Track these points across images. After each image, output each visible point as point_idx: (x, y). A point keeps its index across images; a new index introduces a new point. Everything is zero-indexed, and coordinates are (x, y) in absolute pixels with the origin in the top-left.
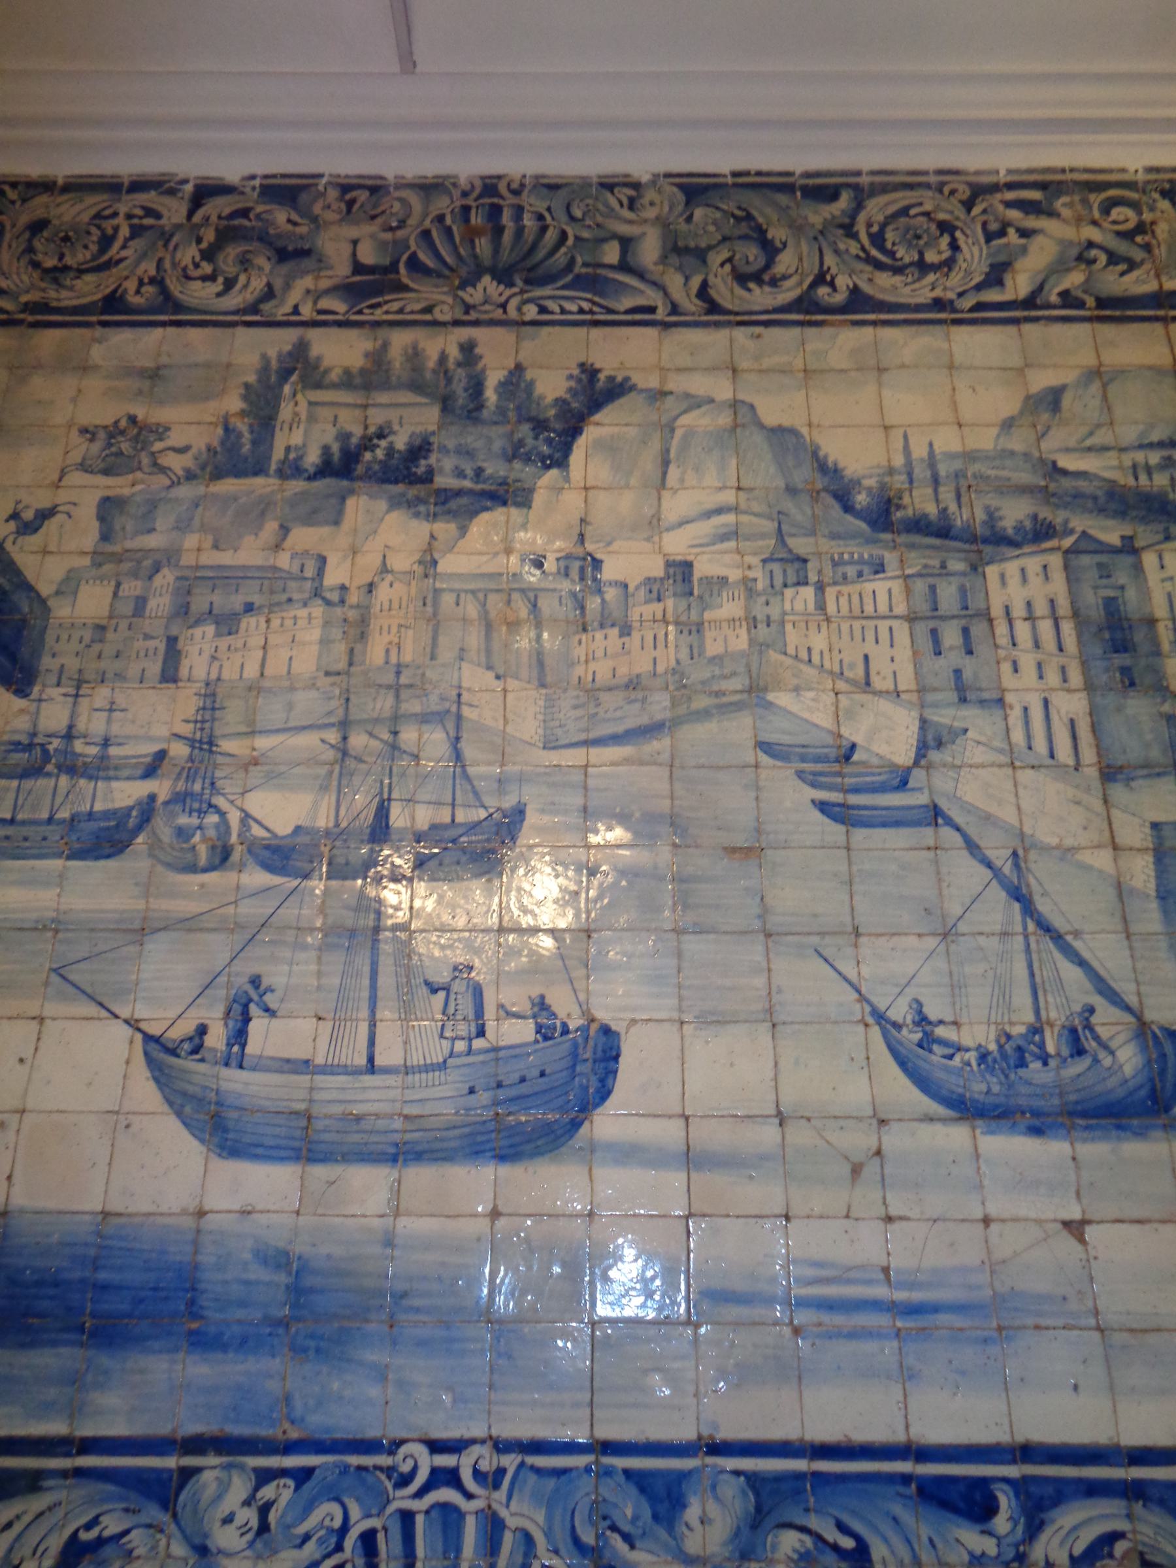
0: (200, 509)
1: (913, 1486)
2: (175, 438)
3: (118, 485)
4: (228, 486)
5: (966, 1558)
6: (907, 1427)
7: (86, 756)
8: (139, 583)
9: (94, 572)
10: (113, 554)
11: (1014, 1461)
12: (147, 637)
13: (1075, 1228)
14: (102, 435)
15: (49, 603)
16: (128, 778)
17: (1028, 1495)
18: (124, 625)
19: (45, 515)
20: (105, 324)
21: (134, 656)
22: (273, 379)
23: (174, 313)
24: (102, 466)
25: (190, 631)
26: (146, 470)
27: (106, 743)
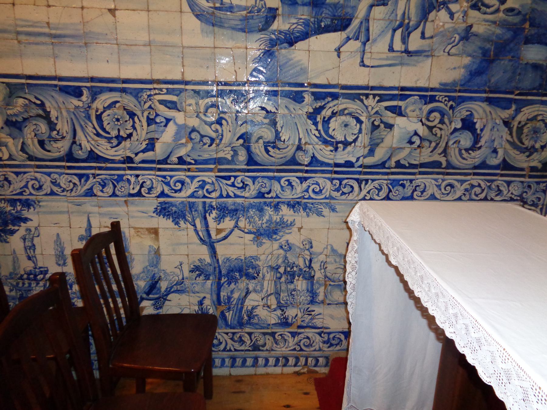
1: (58, 88)
5: (74, 107)
6: (55, 71)
11: (88, 82)
13: (112, 11)
17: (92, 91)
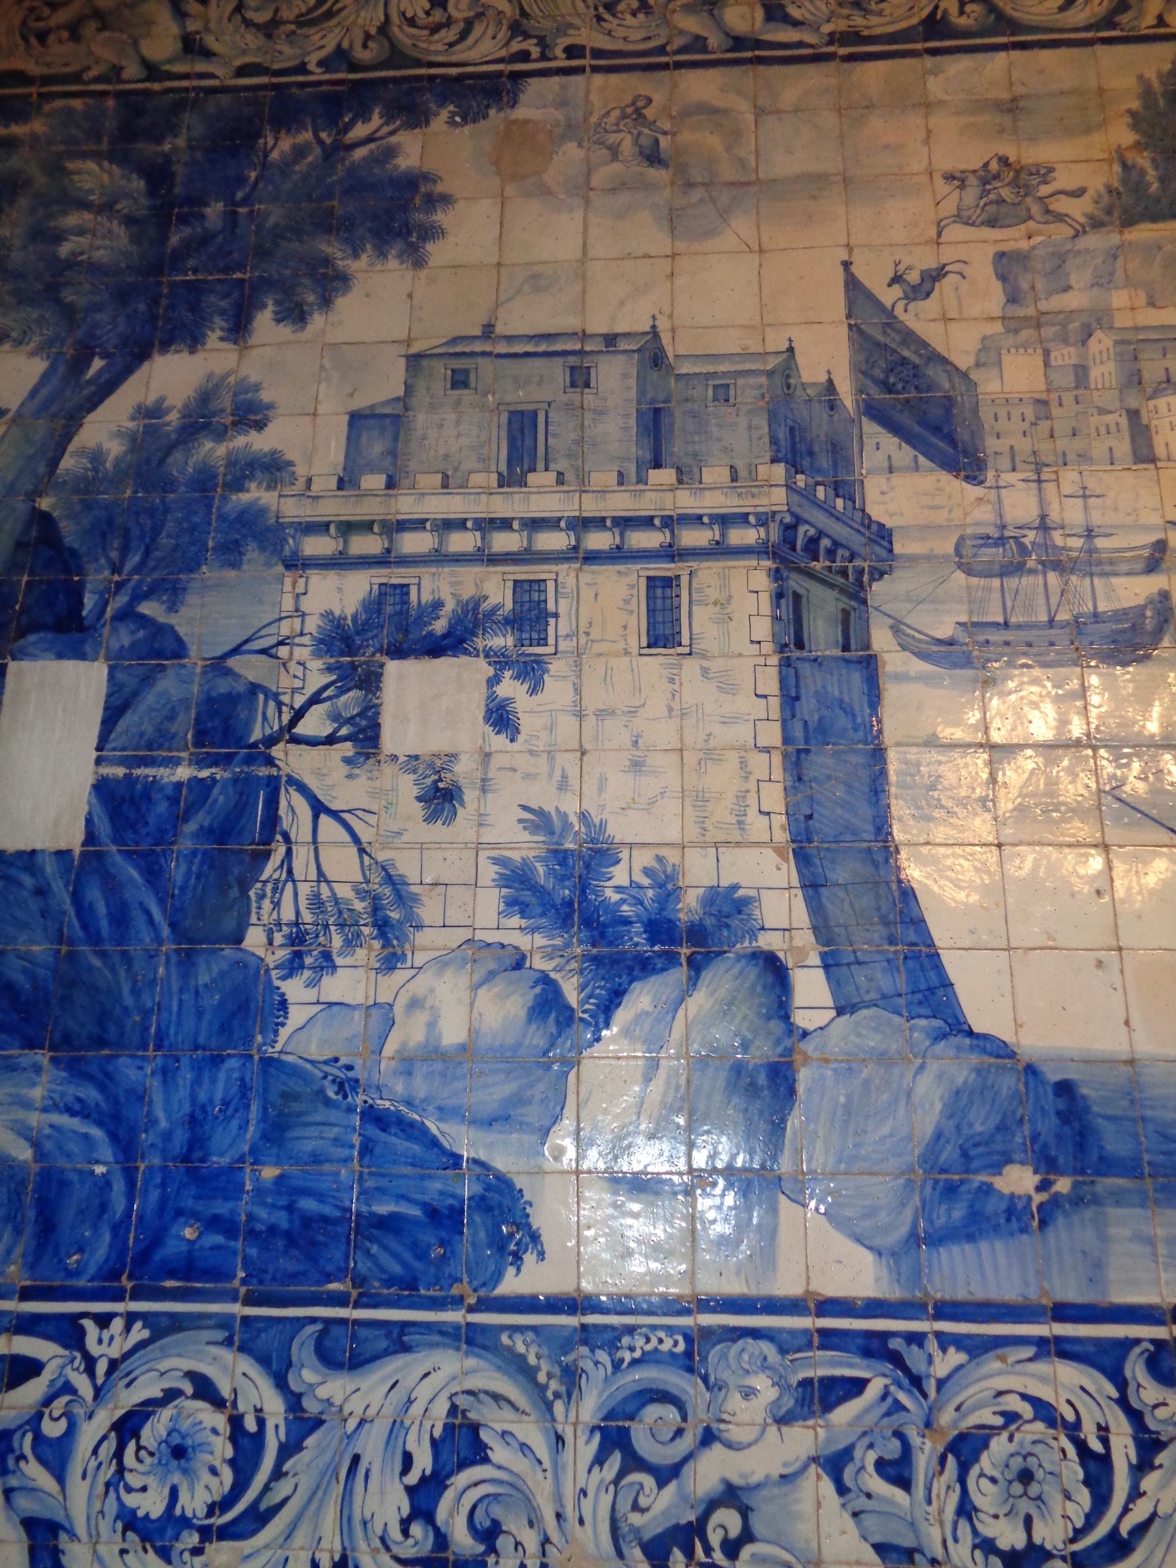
0: (1120, 261)
2: (1064, 179)
3: (1013, 238)
4: (1144, 232)
7: (1071, 549)
8: (1072, 349)
9: (1011, 340)
10: (1026, 319)
12: (1102, 411)
14: (972, 180)
15: (973, 376)
16: (1128, 574)
18: (1068, 398)
19: (936, 275)
20: (934, 52)
21: (1093, 431)
22: (1162, 103)
23: (1012, 34)
24: (984, 217)
25: (1151, 403)
26: (1038, 218)
27: (1090, 534)
